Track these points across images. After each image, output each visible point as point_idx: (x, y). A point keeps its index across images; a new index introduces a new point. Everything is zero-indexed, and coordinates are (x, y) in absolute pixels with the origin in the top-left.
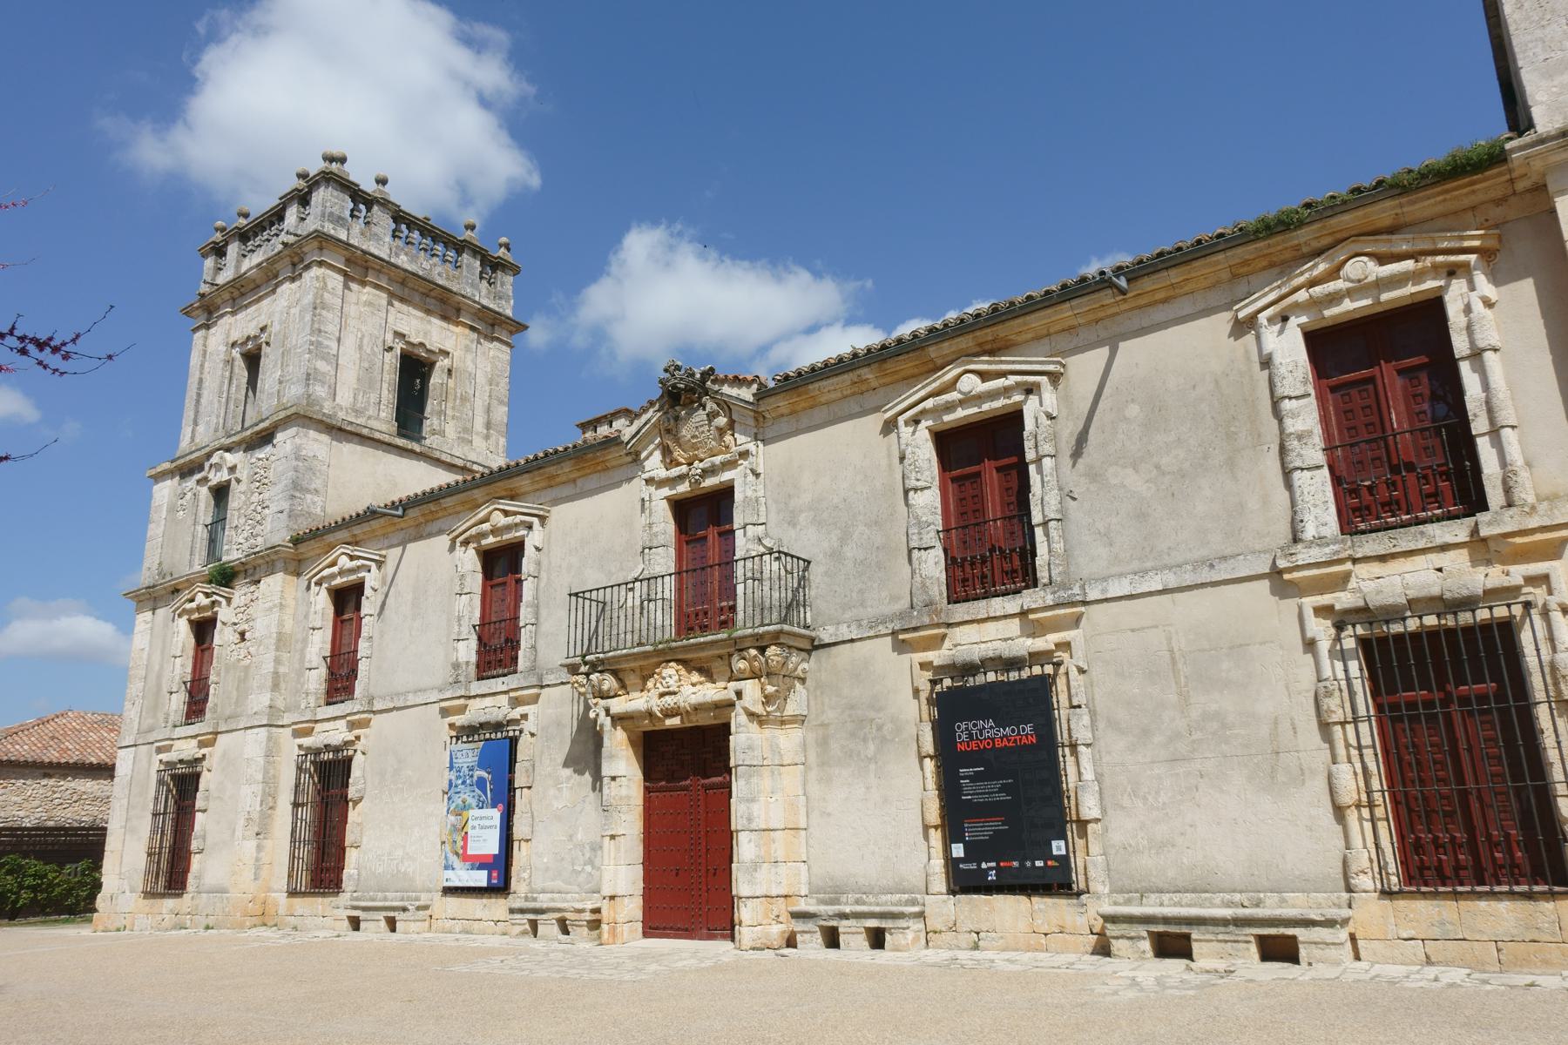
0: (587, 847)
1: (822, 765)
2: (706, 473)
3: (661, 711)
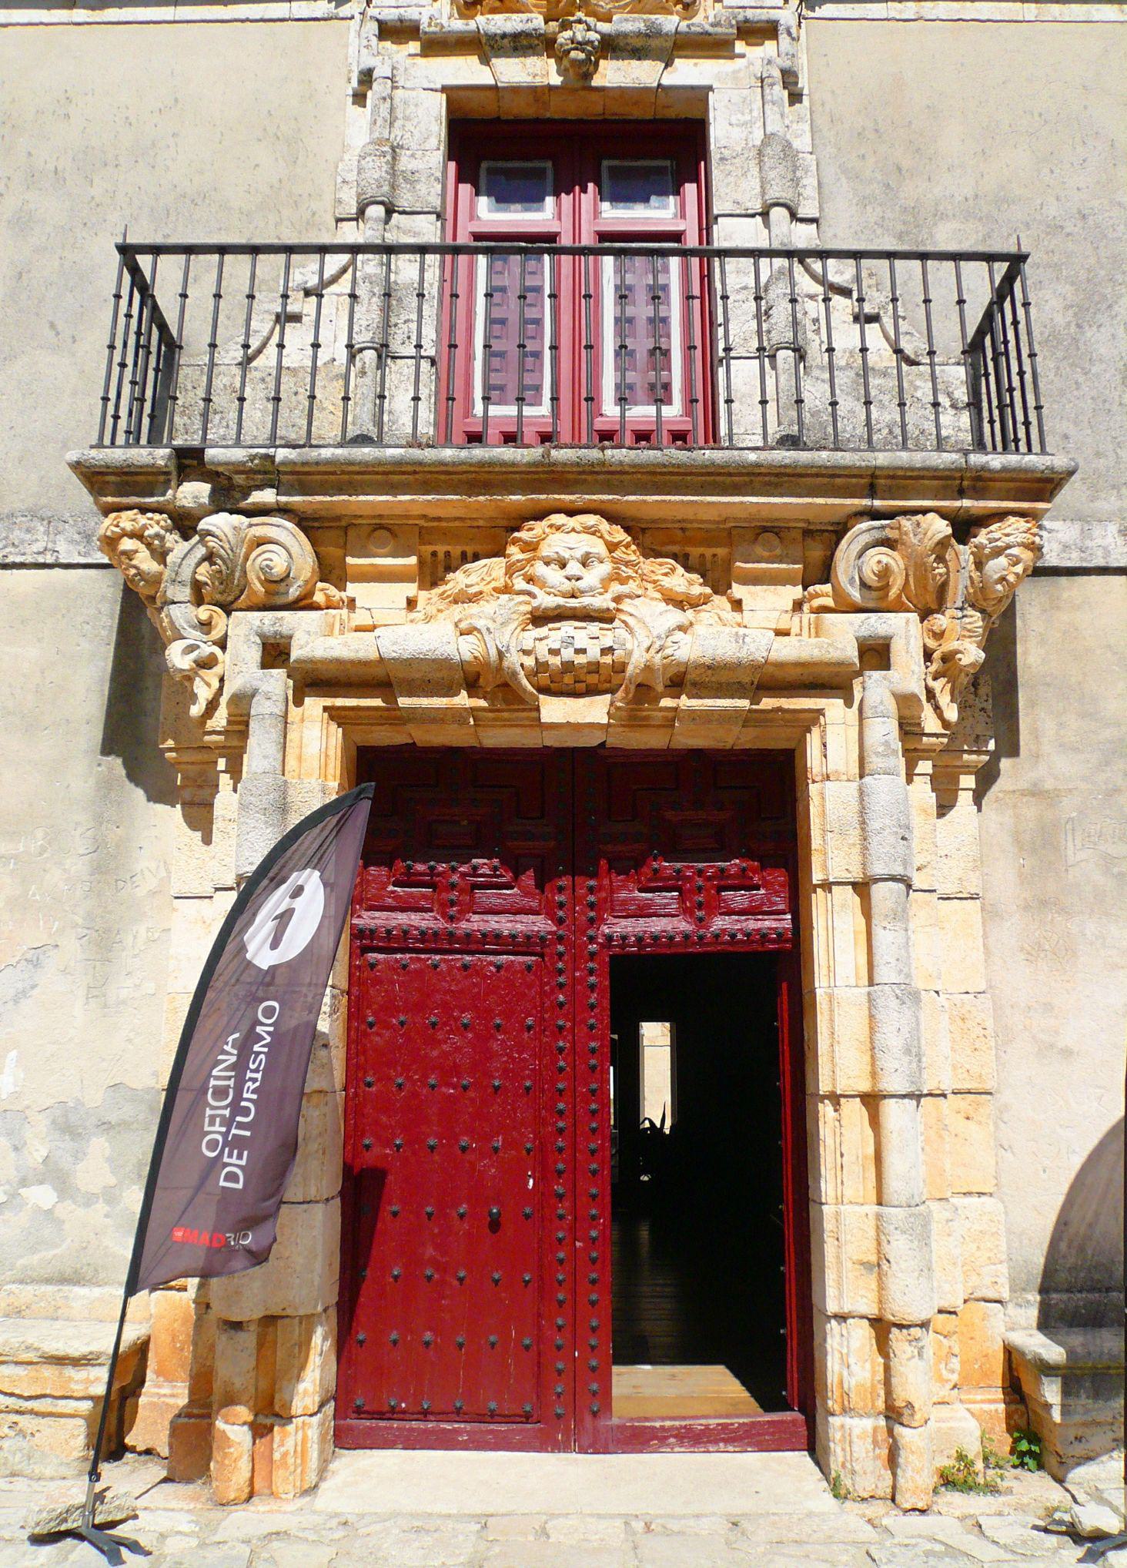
0: (42, 1123)
1: (1041, 905)
2: (612, 47)
3: (532, 675)
